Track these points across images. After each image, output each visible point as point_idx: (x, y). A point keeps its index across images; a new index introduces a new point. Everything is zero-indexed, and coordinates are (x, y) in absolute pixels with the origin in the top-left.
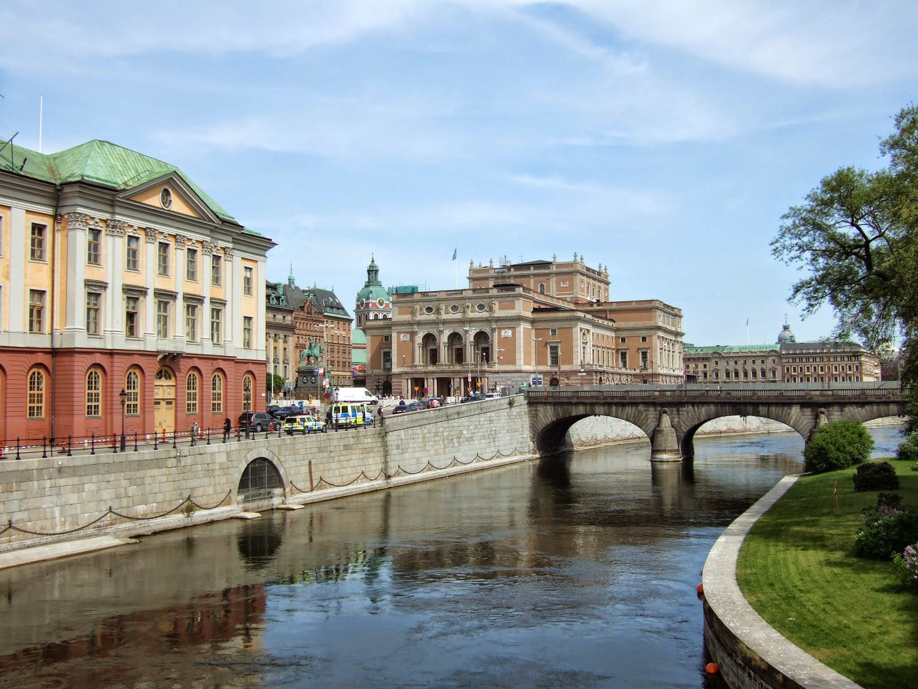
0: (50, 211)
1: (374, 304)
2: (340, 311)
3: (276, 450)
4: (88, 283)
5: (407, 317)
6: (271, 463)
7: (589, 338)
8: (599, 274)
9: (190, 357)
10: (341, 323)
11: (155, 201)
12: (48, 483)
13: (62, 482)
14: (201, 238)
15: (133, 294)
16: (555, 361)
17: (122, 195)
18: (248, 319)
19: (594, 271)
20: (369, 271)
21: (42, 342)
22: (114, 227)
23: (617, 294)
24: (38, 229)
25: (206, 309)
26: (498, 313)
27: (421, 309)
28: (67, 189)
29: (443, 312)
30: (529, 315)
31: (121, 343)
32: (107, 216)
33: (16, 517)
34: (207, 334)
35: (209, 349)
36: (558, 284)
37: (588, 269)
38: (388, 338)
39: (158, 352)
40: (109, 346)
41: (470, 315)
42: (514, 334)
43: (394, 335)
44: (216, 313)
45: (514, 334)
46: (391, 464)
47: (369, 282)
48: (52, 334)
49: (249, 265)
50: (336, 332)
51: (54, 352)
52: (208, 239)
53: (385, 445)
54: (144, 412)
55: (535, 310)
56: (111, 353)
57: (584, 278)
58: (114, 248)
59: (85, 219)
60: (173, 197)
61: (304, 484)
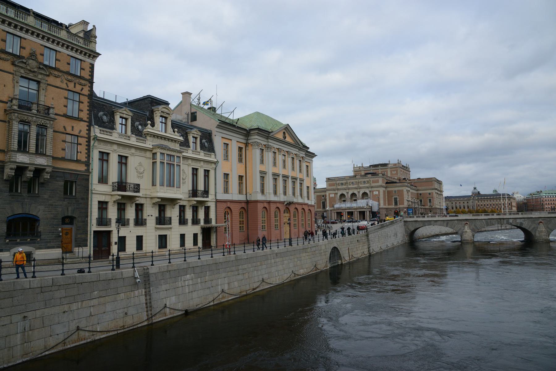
0: (244, 141)
3: (338, 243)
4: (261, 172)
6: (337, 249)
7: (410, 193)
8: (407, 168)
11: (280, 136)
12: (273, 261)
13: (277, 260)
15: (276, 176)
16: (396, 204)
17: (272, 134)
18: (308, 187)
21: (242, 198)
22: (268, 147)
23: (414, 175)
24: (240, 149)
28: (252, 132)
30: (384, 185)
31: (273, 198)
32: (265, 143)
33: (265, 276)
34: (299, 194)
35: (300, 200)
36: (391, 172)
37: (403, 166)
38: (324, 196)
40: (268, 200)
42: (379, 192)
43: (327, 195)
44: (301, 184)
45: (379, 192)
46: (371, 248)
48: (246, 194)
49: (308, 164)
51: (247, 202)
53: (368, 240)
54: (280, 228)
55: (387, 183)
56: (269, 202)
59: (258, 144)
60: (287, 135)
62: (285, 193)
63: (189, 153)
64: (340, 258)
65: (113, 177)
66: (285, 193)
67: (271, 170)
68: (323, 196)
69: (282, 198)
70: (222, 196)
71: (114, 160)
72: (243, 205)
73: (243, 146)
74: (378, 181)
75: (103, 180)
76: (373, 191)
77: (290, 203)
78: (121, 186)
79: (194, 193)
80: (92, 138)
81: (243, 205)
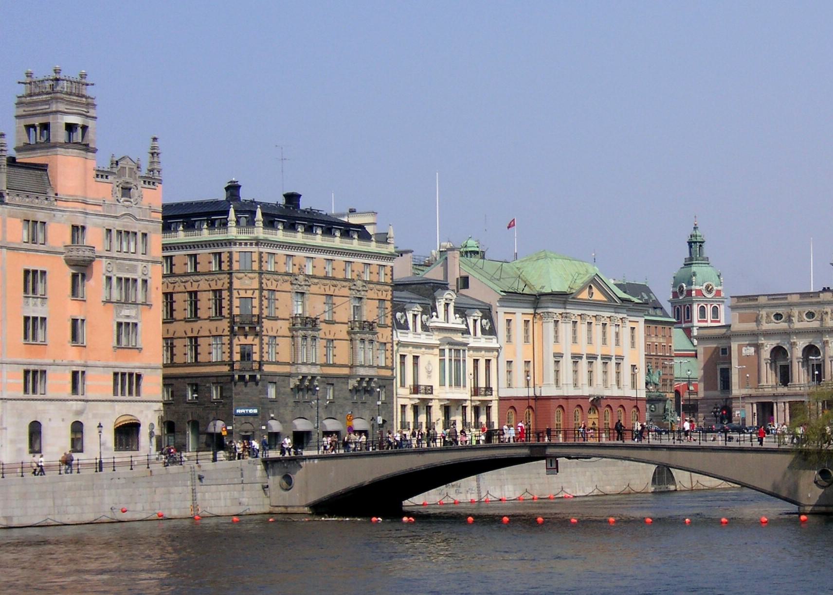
1: (699, 292)
2: (658, 312)
5: (751, 326)
9: (608, 398)
10: (660, 326)
11: (585, 295)
12: (573, 470)
14: (609, 314)
15: (576, 358)
18: (634, 367)
20: (690, 243)
22: (565, 316)
24: (527, 322)
25: (612, 364)
27: (768, 316)
28: (543, 298)
29: (795, 319)
31: (571, 392)
34: (614, 382)
35: (615, 392)
38: (726, 352)
39: (590, 396)
43: (734, 346)
44: (618, 364)
47: (691, 259)
50: (654, 340)
51: (536, 398)
52: (613, 314)
56: (567, 398)
58: (566, 329)
60: (594, 290)
62: (590, 383)
64: (674, 483)
65: (409, 381)
66: (590, 383)
68: (724, 351)
69: (586, 391)
70: (503, 394)
71: (409, 361)
73: (530, 318)
75: (403, 385)
78: (416, 389)
79: (476, 391)
80: (395, 343)
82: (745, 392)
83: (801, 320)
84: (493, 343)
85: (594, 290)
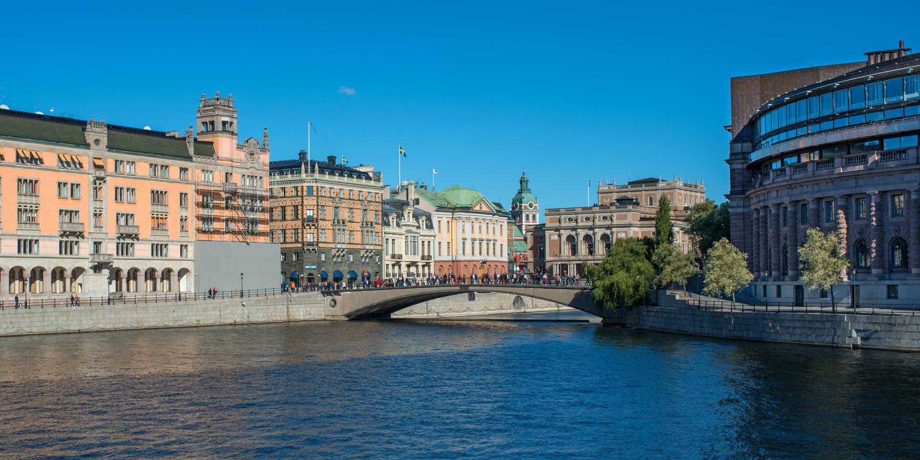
1: (525, 207)
5: (557, 225)
11: (477, 208)
15: (473, 240)
19: (690, 186)
20: (521, 182)
21: (450, 258)
25: (491, 243)
26: (615, 222)
29: (579, 221)
41: (597, 223)
57: (683, 192)
60: (483, 205)
61: (530, 306)
62: (480, 254)
63: (422, 232)
64: (524, 305)
65: (390, 253)
66: (480, 254)
67: (468, 235)
69: (477, 257)
70: (438, 258)
71: (390, 241)
72: (451, 264)
74: (625, 218)
76: (617, 233)
77: (484, 262)
78: (393, 256)
79: (423, 258)
81: (451, 264)
82: (552, 258)
83: (582, 221)
84: (431, 233)
85: (483, 205)
